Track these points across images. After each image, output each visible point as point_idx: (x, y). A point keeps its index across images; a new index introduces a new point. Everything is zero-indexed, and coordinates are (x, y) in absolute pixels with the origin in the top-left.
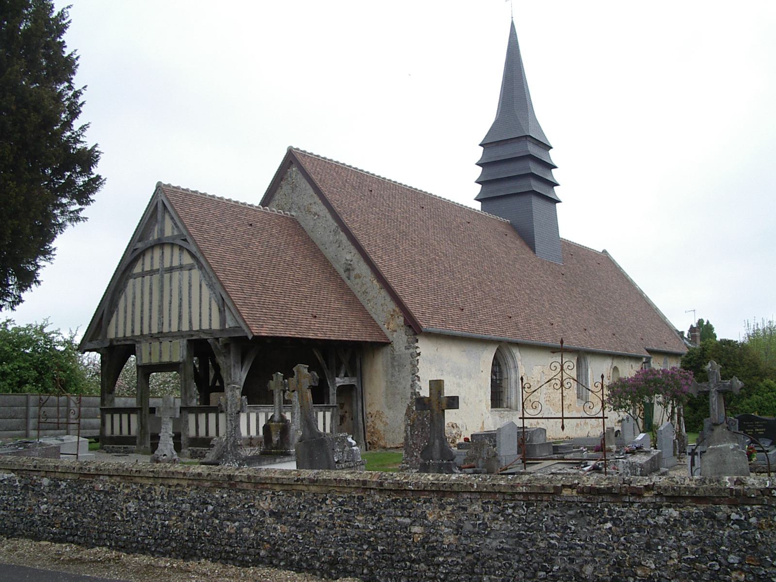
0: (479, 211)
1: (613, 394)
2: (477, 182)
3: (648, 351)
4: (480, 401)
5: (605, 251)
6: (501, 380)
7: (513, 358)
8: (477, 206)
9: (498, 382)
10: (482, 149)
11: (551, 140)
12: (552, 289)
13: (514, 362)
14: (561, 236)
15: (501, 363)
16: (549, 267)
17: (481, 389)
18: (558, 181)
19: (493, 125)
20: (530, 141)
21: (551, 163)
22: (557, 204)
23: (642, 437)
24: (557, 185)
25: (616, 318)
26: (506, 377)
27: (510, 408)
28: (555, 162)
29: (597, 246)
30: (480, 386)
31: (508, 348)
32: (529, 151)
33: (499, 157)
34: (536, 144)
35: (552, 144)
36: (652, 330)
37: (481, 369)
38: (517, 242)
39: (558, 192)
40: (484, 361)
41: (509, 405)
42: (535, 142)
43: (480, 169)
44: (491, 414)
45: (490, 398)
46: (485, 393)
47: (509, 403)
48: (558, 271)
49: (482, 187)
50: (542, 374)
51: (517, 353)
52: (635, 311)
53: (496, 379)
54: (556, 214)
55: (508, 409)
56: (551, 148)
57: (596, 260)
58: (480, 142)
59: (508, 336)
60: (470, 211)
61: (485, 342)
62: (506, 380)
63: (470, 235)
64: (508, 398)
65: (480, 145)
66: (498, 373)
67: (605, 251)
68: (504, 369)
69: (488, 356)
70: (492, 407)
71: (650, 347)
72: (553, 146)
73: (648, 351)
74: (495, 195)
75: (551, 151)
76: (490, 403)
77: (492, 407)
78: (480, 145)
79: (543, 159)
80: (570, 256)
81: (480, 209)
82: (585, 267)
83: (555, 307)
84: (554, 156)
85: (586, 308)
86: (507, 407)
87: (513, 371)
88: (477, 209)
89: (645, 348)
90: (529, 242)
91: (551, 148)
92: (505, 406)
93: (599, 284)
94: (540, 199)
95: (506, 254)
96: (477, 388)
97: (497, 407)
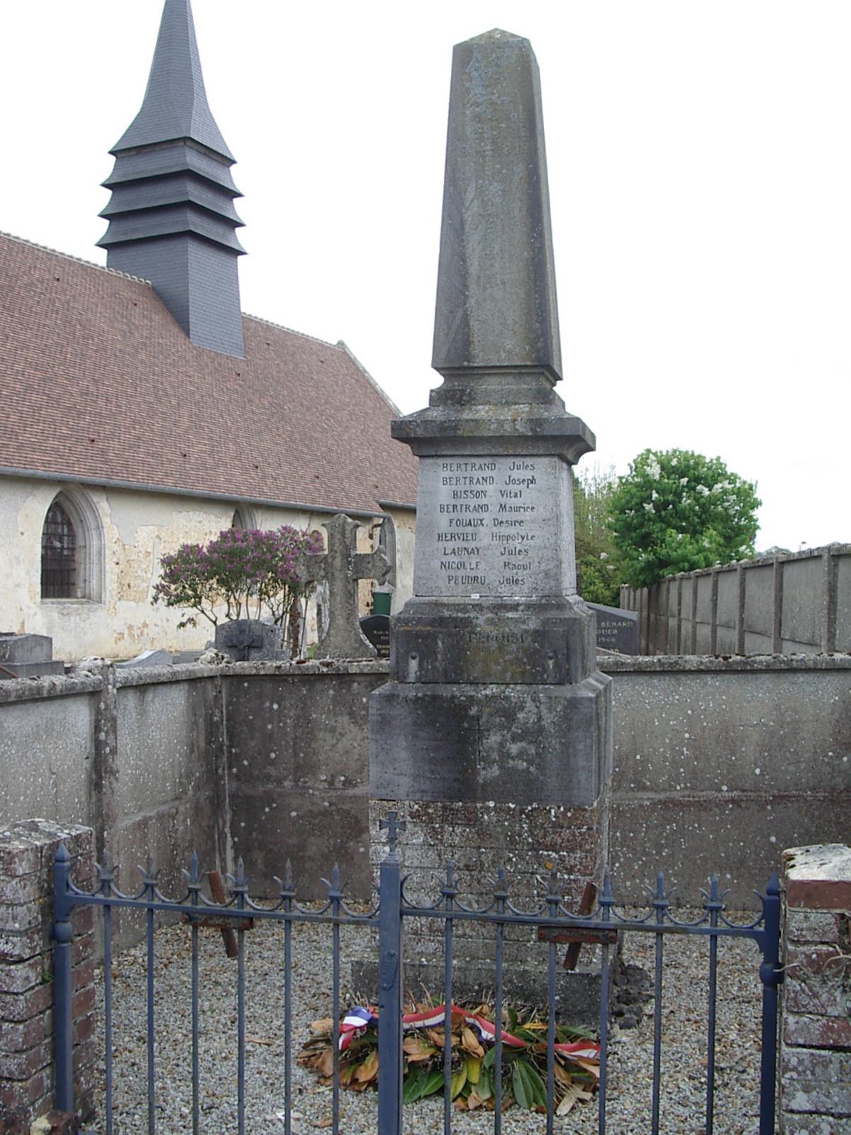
0: (103, 268)
1: (172, 577)
2: (103, 216)
3: (383, 506)
4: (17, 585)
5: (341, 344)
6: (73, 549)
7: (94, 511)
8: (100, 258)
9: (66, 553)
10: (113, 159)
11: (234, 147)
12: (207, 399)
13: (97, 518)
14: (242, 311)
15: (72, 520)
16: (213, 362)
17: (19, 562)
18: (243, 219)
19: (136, 119)
20: (190, 148)
21: (233, 189)
22: (240, 258)
23: (147, 656)
24: (241, 225)
25: (330, 450)
26: (82, 544)
27: (90, 598)
28: (239, 186)
29: (328, 335)
30: (17, 558)
31: (84, 495)
32: (186, 164)
33: (138, 173)
34: (205, 154)
35: (235, 156)
36: (403, 472)
37: (21, 530)
38: (157, 318)
39: (242, 237)
40: (27, 516)
41: (87, 592)
42: (203, 150)
43: (109, 193)
44: (41, 609)
45: (39, 580)
46: (28, 573)
47: (87, 588)
48: (230, 369)
49: (110, 225)
50: (157, 540)
51: (103, 504)
52: (375, 441)
53: (62, 548)
54: (237, 273)
55: (85, 600)
56: (234, 162)
57: (318, 356)
58: (111, 147)
59: (80, 472)
60: (85, 269)
61: (34, 482)
62: (83, 551)
63: (52, 301)
64: (85, 581)
65: (111, 153)
66: (66, 538)
67: (341, 344)
68: (79, 531)
69: (37, 506)
70: (42, 597)
71: (389, 501)
72: (236, 160)
73: (383, 506)
74: (128, 238)
75: (233, 168)
76: (39, 589)
77: (46, 593)
78: (111, 153)
79: (222, 183)
80: (265, 346)
81: (104, 264)
82: (291, 366)
83: (202, 428)
84: (238, 177)
85: (271, 431)
86: (84, 597)
87: (94, 533)
88: (100, 265)
89: (377, 502)
90: (181, 318)
91: (234, 162)
92: (79, 594)
93: (313, 394)
94: (204, 247)
95: (124, 336)
96: (11, 562)
97: (62, 597)
